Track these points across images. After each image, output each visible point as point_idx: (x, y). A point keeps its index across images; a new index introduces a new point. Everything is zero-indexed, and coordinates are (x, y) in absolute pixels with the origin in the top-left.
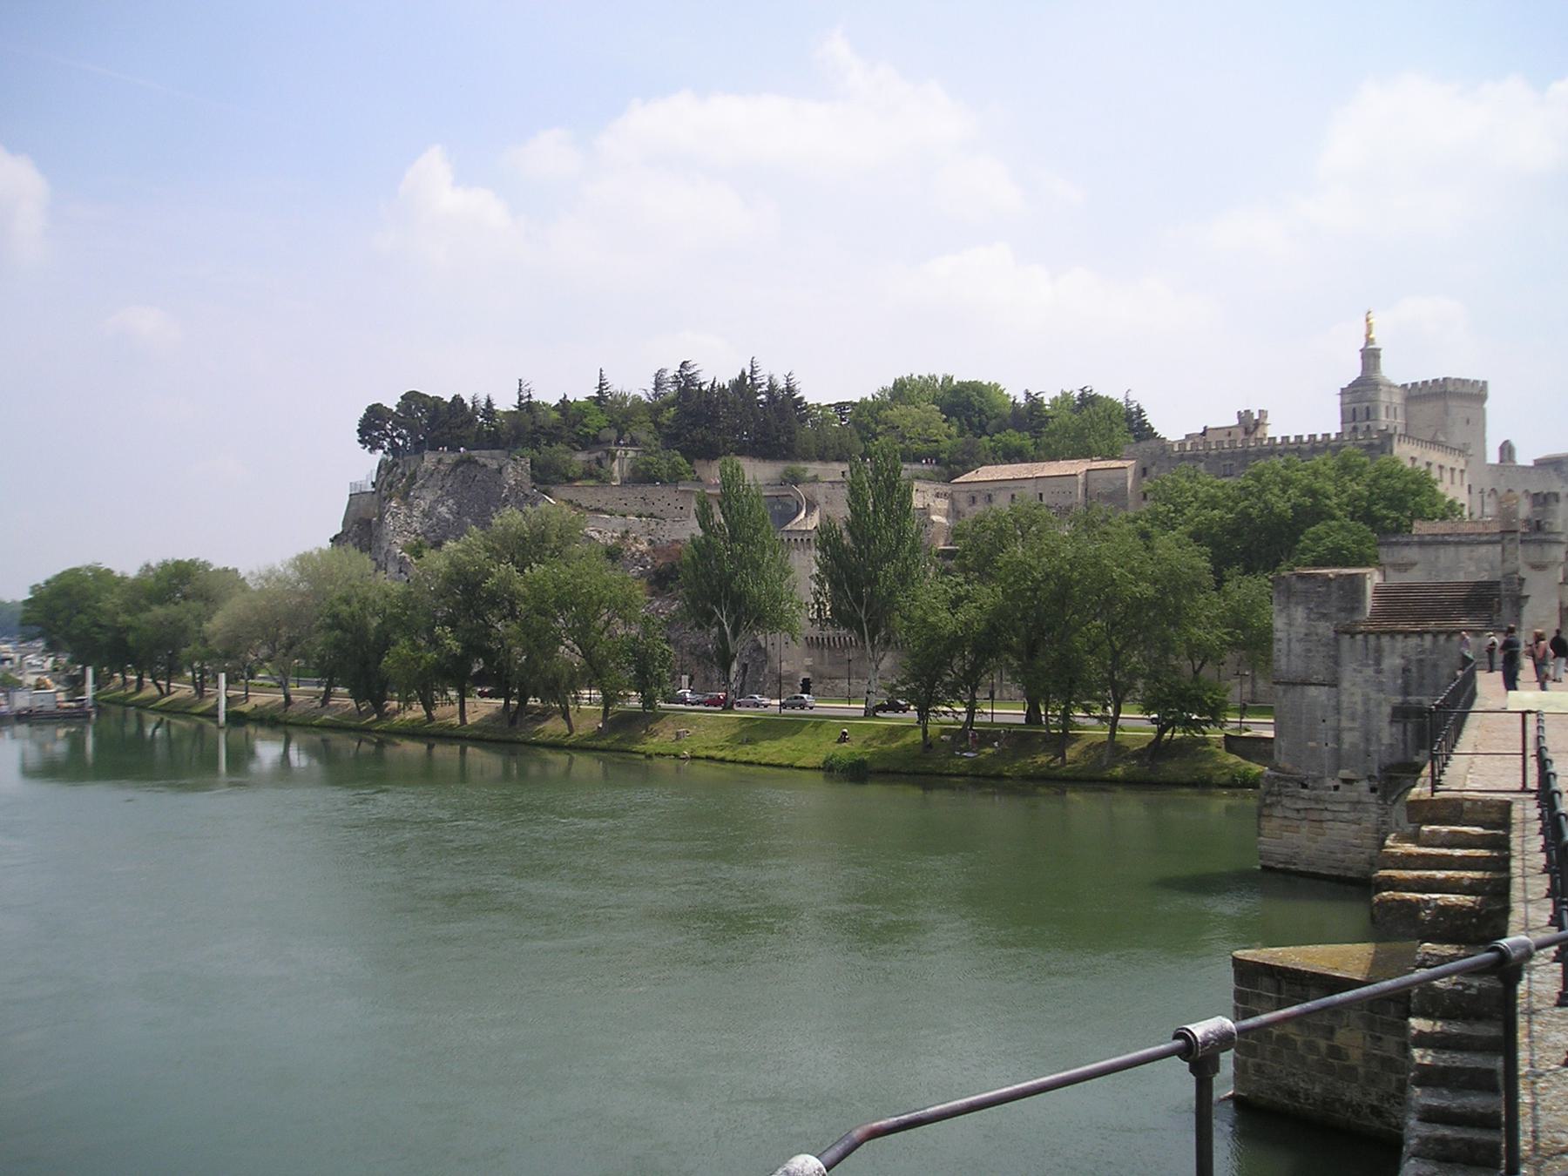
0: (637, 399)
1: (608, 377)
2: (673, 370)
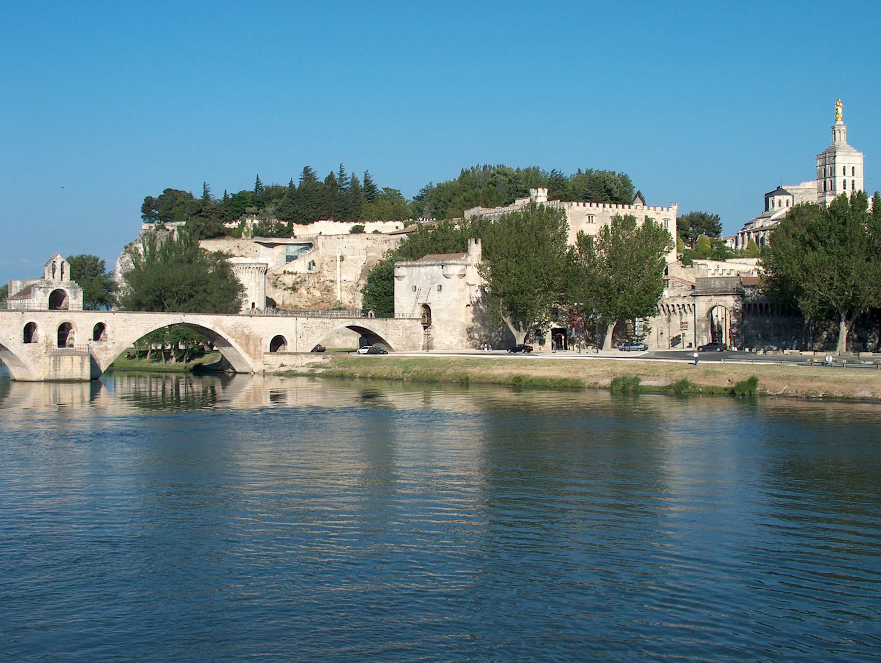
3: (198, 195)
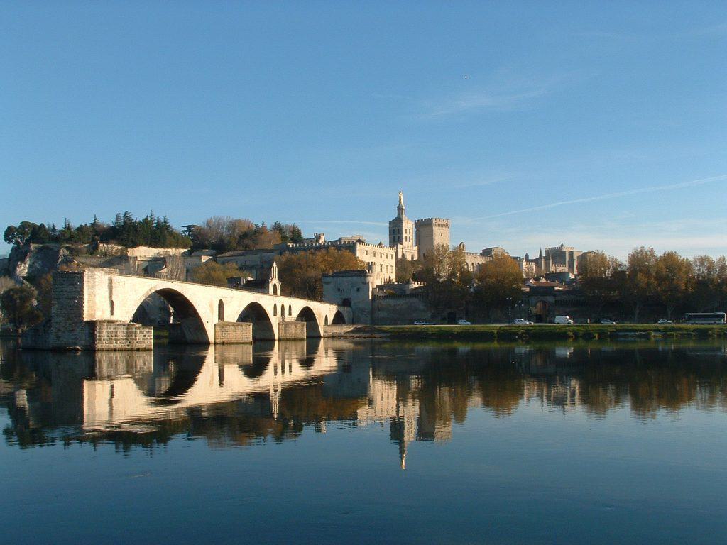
2: (122, 215)
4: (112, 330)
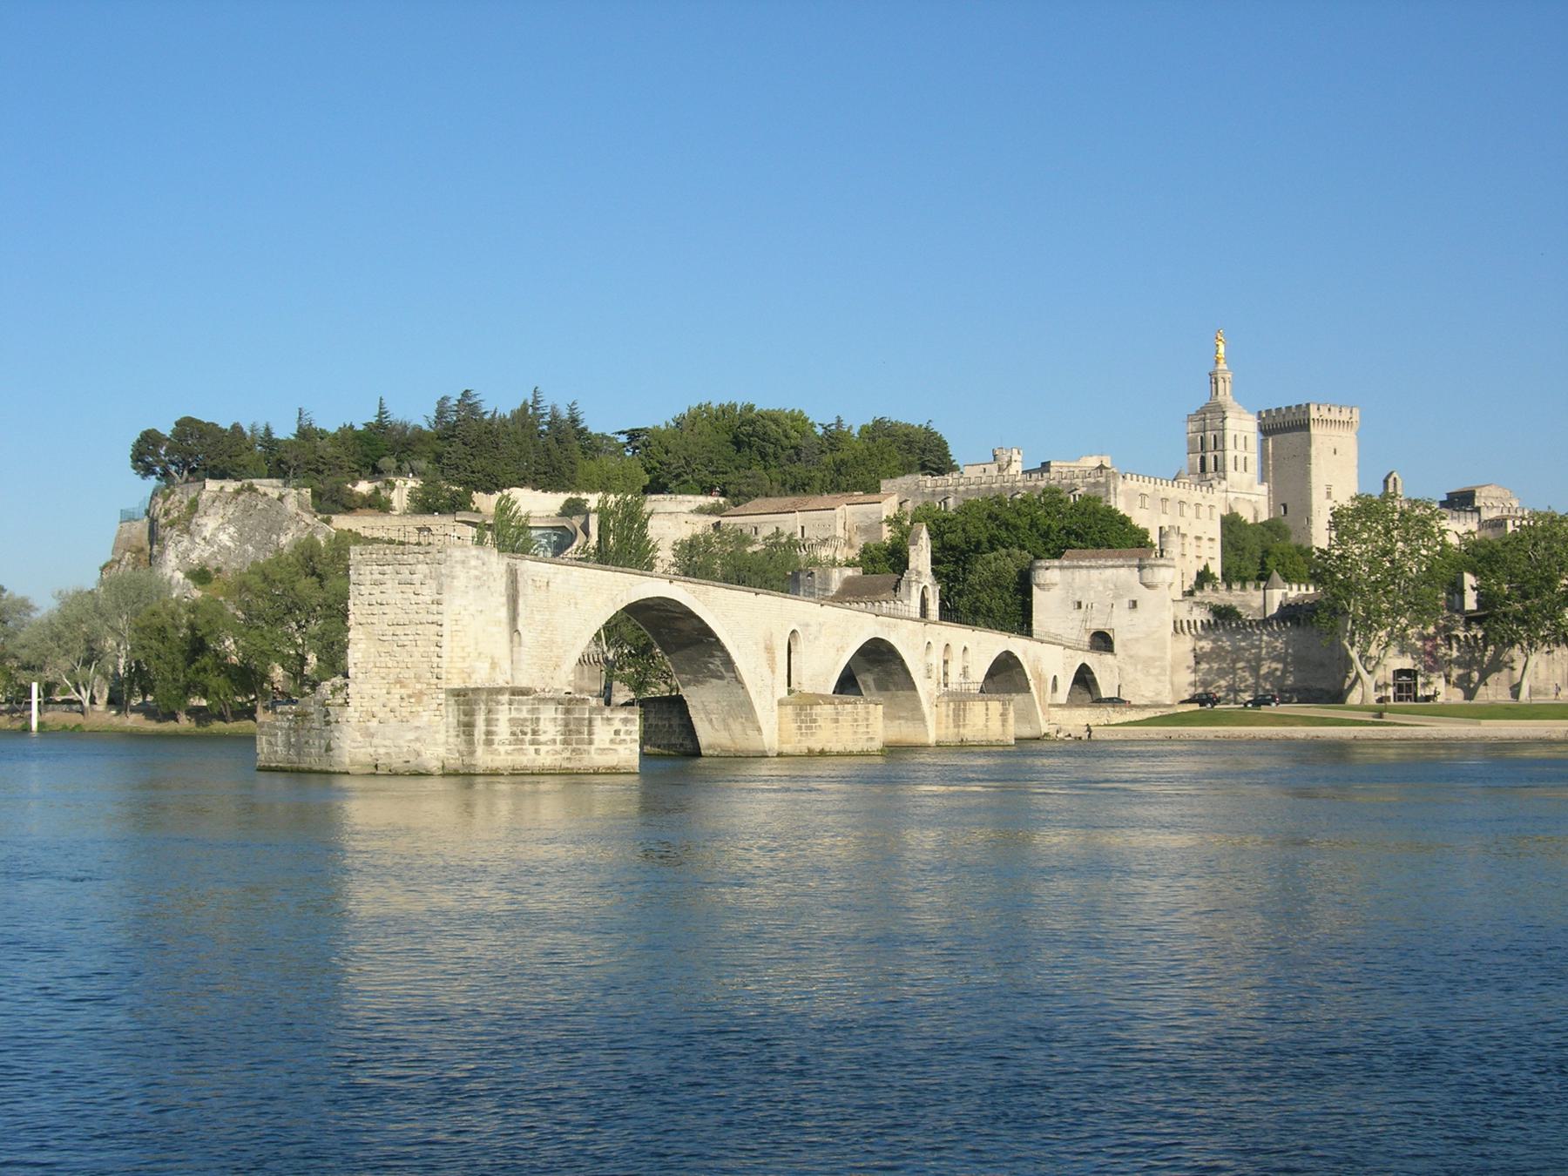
0: (418, 429)
1: (388, 406)
3: (285, 431)
4: (524, 714)
